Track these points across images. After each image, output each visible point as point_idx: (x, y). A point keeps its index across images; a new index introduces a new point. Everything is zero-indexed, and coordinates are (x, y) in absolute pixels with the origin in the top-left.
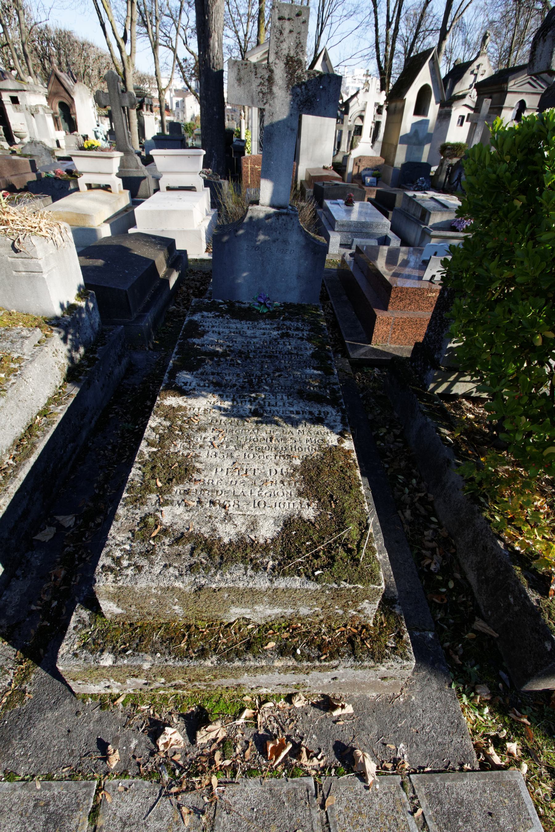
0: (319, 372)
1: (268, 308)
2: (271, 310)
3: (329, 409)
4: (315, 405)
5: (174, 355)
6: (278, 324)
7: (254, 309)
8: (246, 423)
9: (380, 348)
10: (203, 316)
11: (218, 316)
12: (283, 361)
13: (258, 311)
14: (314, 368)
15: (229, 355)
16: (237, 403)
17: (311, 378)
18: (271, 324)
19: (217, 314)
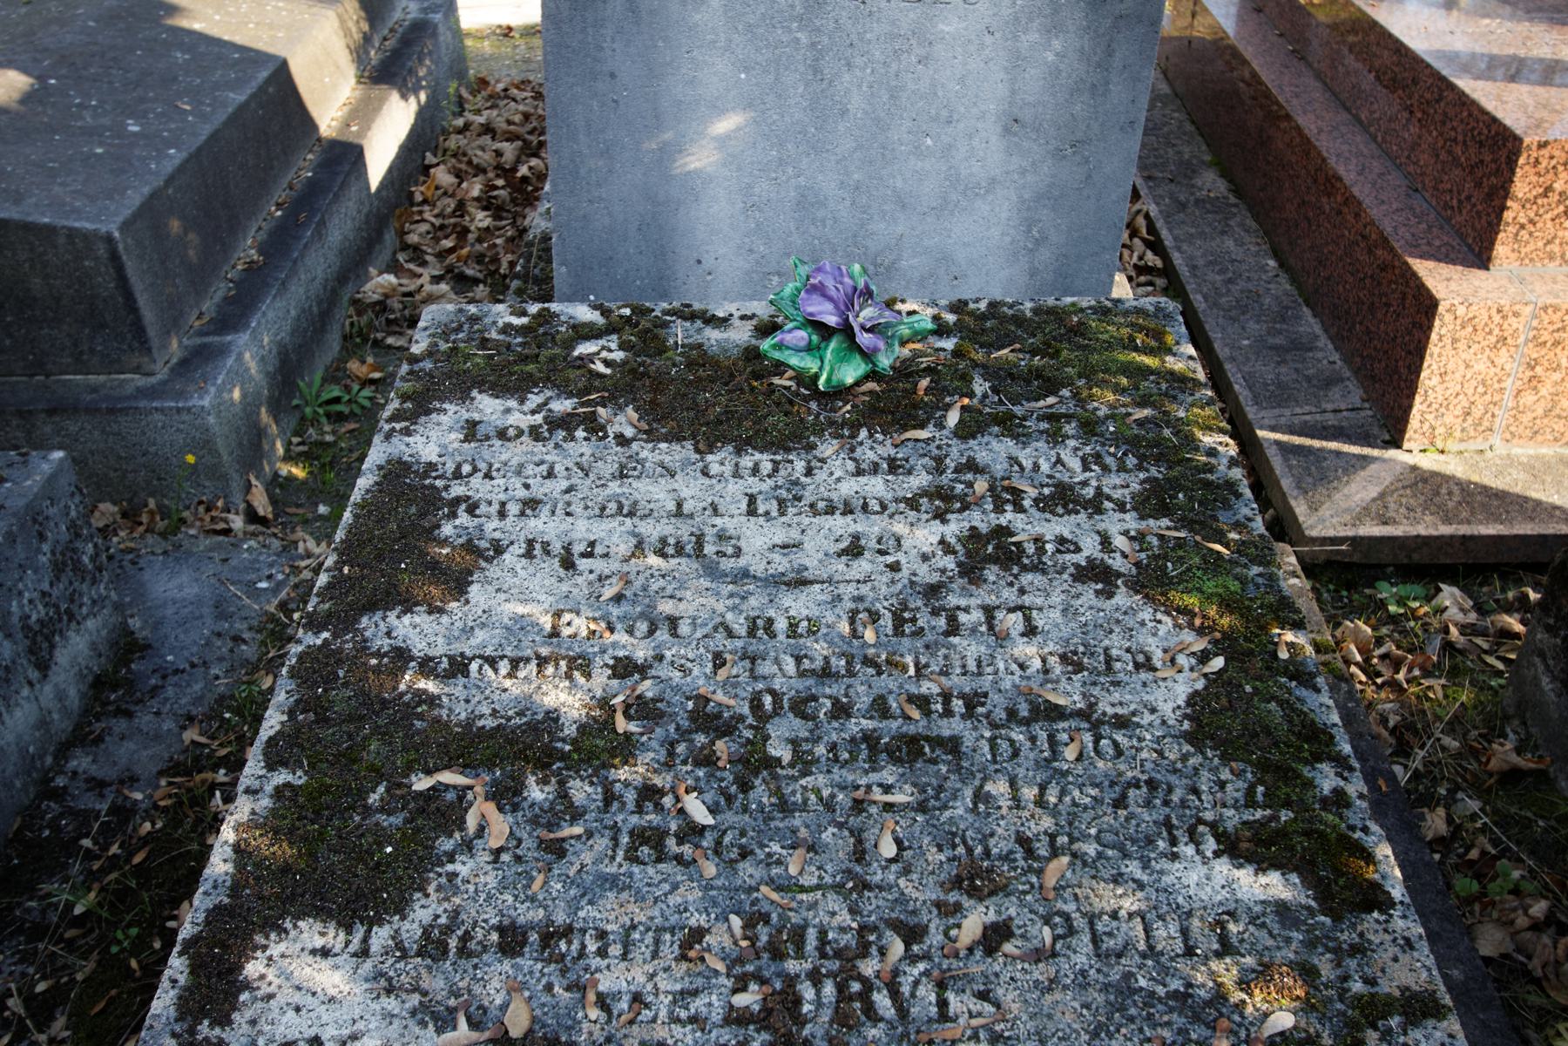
0: (1275, 886)
1: (867, 355)
2: (884, 362)
5: (254, 766)
6: (939, 469)
7: (779, 368)
9: (1453, 466)
10: (471, 430)
11: (565, 423)
13: (807, 380)
14: (1233, 847)
15: (626, 749)
17: (1226, 948)
18: (894, 466)
19: (563, 406)
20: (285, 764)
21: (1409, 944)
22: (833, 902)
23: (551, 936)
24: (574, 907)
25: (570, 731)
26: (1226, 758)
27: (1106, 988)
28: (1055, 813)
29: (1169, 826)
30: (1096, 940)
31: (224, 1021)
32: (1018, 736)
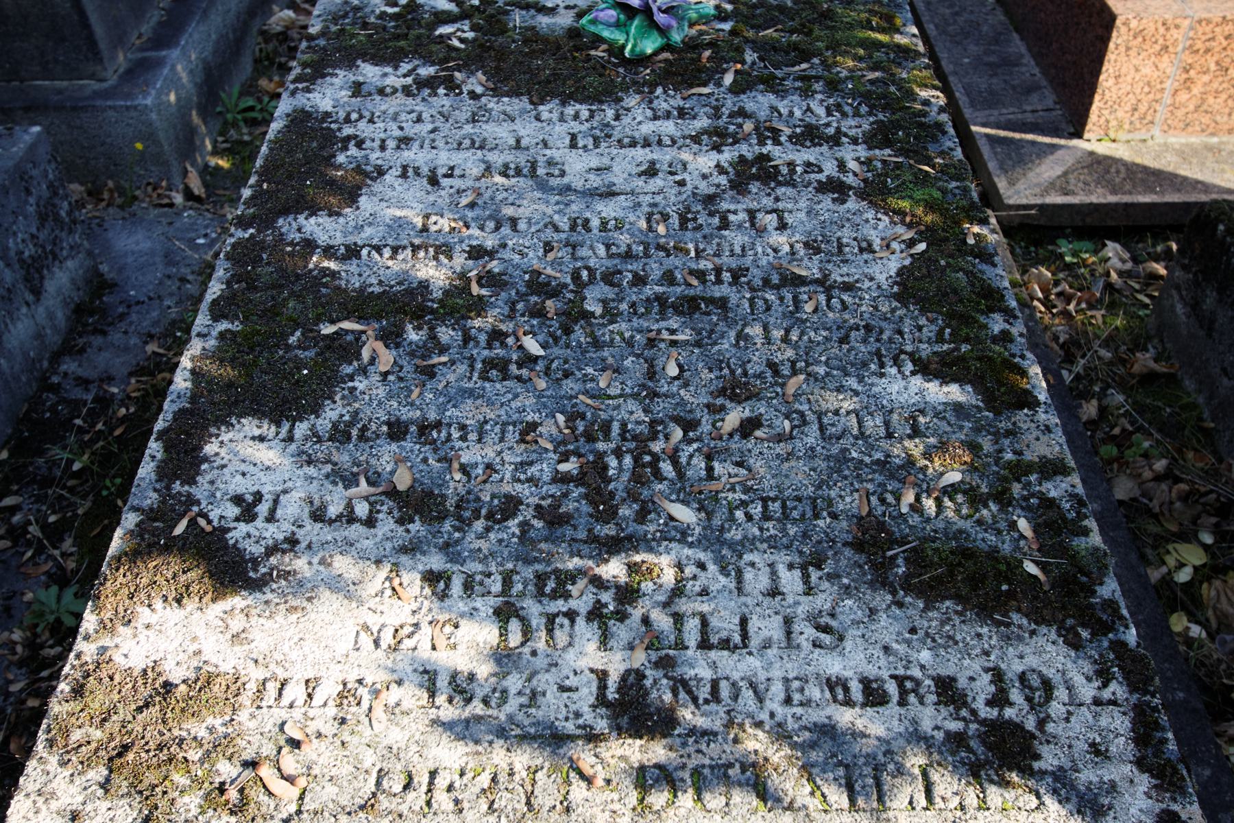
0: (955, 392)
1: (663, 31)
2: (676, 37)
3: (1045, 653)
4: (964, 633)
5: (202, 320)
6: (717, 115)
7: (597, 40)
8: (578, 791)
9: (1121, 152)
10: (357, 89)
11: (430, 84)
12: (755, 331)
13: (616, 51)
14: (924, 369)
15: (479, 307)
16: (527, 633)
17: (916, 432)
18: (682, 113)
19: (427, 71)
20: (225, 317)
21: (1048, 429)
22: (632, 405)
23: (424, 429)
24: (442, 409)
25: (437, 294)
26: (923, 311)
27: (828, 458)
28: (796, 347)
29: (878, 354)
30: (822, 428)
31: (192, 481)
32: (771, 296)
